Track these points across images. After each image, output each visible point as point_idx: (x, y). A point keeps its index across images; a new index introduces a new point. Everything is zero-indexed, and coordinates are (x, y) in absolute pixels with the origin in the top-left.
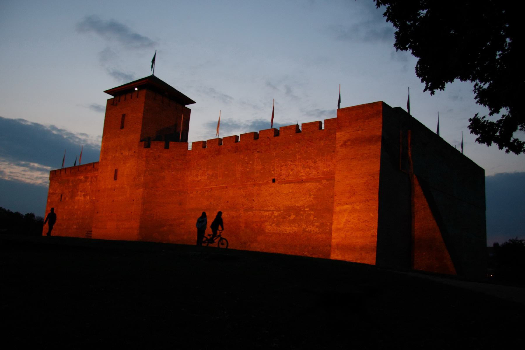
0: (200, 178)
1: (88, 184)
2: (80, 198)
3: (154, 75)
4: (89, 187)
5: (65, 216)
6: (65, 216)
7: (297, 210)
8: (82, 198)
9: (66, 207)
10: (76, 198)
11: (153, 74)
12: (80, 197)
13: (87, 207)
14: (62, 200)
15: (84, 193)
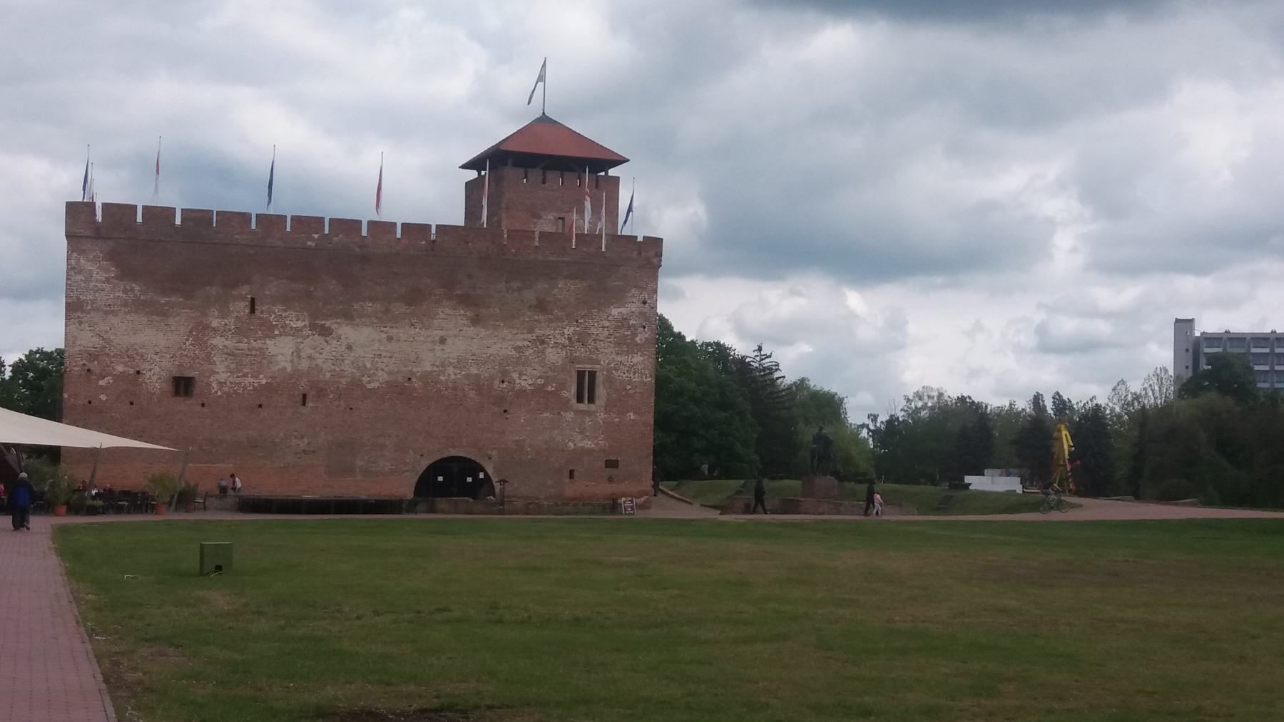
11: (544, 113)
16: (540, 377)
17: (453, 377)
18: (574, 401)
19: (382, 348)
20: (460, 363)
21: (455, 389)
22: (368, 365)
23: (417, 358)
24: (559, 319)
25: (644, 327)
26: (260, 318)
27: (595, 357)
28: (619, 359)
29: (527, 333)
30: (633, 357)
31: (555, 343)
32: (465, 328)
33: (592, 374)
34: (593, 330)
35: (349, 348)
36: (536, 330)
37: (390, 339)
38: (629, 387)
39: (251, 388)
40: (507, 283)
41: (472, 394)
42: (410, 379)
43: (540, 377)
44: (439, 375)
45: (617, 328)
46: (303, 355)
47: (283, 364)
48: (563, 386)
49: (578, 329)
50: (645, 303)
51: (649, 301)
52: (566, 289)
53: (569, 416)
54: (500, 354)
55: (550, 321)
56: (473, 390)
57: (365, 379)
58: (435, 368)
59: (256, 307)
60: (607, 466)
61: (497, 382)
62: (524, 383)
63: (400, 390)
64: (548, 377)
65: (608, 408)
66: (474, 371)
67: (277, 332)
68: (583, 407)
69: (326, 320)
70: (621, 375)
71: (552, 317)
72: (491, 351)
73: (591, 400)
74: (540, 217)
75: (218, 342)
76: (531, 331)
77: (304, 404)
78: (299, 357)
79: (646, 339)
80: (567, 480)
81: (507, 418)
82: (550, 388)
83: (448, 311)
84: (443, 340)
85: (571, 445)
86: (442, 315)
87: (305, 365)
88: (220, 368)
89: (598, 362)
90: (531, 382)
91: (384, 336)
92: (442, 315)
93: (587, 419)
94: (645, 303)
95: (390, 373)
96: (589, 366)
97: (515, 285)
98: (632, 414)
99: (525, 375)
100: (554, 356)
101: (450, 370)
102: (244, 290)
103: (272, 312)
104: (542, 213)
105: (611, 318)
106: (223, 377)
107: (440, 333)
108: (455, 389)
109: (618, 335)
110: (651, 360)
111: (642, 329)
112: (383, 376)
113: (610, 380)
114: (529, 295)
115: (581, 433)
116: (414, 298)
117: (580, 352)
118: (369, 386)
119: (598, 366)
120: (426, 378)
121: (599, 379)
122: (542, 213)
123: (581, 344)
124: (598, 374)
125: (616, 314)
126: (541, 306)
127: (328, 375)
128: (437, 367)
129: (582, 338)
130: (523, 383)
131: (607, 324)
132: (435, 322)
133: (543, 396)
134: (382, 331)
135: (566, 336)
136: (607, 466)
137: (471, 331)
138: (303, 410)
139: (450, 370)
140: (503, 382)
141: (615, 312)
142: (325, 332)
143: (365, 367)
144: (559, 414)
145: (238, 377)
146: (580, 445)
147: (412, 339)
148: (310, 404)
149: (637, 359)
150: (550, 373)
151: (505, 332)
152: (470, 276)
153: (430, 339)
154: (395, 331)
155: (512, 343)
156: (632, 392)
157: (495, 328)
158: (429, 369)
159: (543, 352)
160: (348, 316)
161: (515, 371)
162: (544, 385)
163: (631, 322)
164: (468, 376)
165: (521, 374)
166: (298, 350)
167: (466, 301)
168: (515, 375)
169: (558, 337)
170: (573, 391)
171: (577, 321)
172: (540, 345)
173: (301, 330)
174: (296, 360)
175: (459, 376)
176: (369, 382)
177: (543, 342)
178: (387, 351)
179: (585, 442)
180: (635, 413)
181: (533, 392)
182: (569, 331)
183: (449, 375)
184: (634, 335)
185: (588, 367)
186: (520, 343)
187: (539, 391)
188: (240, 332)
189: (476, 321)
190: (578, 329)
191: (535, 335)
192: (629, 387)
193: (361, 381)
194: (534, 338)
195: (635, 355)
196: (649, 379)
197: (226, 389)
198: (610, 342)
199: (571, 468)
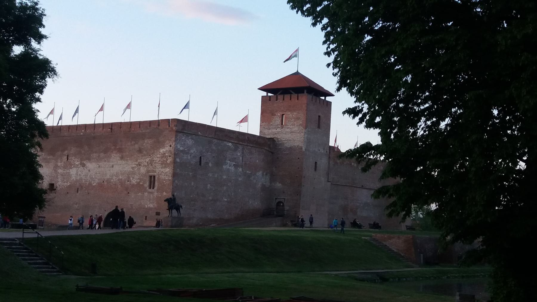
1: (239, 154)
2: (229, 166)
3: (299, 71)
4: (241, 158)
5: (209, 185)
6: (209, 185)
8: (233, 168)
9: (210, 175)
10: (224, 167)
11: (298, 71)
12: (230, 166)
13: (240, 179)
14: (202, 165)
15: (234, 163)
16: (139, 179)
17: (115, 180)
18: (148, 188)
19: (97, 170)
20: (117, 175)
21: (115, 185)
22: (94, 177)
23: (106, 173)
24: (145, 155)
25: (170, 156)
26: (69, 162)
27: (155, 170)
28: (162, 170)
29: (136, 162)
30: (166, 169)
31: (144, 165)
32: (119, 161)
33: (154, 176)
34: (155, 159)
35: (89, 171)
36: (138, 160)
37: (99, 167)
38: (164, 182)
39: (66, 187)
40: (131, 142)
41: (119, 187)
42: (104, 181)
43: (139, 179)
44: (111, 180)
45: (162, 157)
46: (78, 174)
47: (73, 178)
49: (150, 159)
50: (171, 146)
51: (172, 146)
52: (148, 143)
53: (146, 194)
54: (128, 170)
55: (142, 156)
56: (119, 185)
57: (93, 182)
58: (110, 177)
59: (68, 158)
60: (156, 215)
61: (126, 181)
62: (134, 182)
63: (101, 185)
64: (140, 179)
65: (158, 190)
66: (120, 177)
67: (72, 167)
68: (150, 190)
69: (84, 161)
70: (162, 177)
71: (143, 154)
72: (125, 169)
73: (153, 188)
74: (275, 115)
75: (60, 171)
76: (137, 161)
77: (78, 192)
78: (77, 175)
79: (171, 161)
80: (144, 220)
81: (129, 196)
82: (141, 183)
83: (114, 155)
84: (113, 166)
85: (146, 206)
86: (113, 157)
87: (78, 178)
88: (59, 180)
90: (136, 181)
91: (98, 166)
92: (113, 157)
93: (151, 195)
94: (171, 146)
95: (99, 179)
96: (153, 174)
97: (133, 143)
98: (165, 193)
99: (135, 178)
100: (143, 170)
101: (114, 178)
102: (66, 152)
103: (72, 159)
104: (276, 113)
105: (160, 153)
106: (60, 183)
107: (112, 163)
108: (115, 185)
109: (162, 160)
110: (172, 170)
111: (169, 157)
112: (97, 181)
113: (159, 179)
114: (137, 146)
115: (149, 201)
116: (106, 151)
117: (151, 168)
118: (93, 185)
119: (155, 174)
120: (108, 181)
121: (156, 178)
122: (276, 113)
123: (151, 165)
124: (156, 177)
125: (162, 151)
126: (140, 151)
127: (84, 181)
128: (111, 176)
129: (151, 163)
130: (134, 182)
131: (159, 156)
132: (111, 159)
133: (139, 187)
134: (97, 164)
135: (147, 162)
136: (156, 215)
137: (120, 162)
138: (78, 194)
139: (114, 178)
140: (128, 181)
141: (162, 151)
142: (84, 165)
143: (93, 177)
144: (143, 193)
145: (63, 183)
146: (149, 206)
147: (105, 166)
148: (79, 192)
149: (167, 170)
150: (141, 177)
151: (130, 162)
152: (121, 141)
153: (109, 166)
154: (100, 163)
155: (131, 166)
156: (165, 183)
157: (127, 160)
158: (109, 178)
159: (140, 169)
160: (89, 159)
161: (131, 177)
162: (140, 182)
163: (166, 155)
164: (119, 179)
165: (133, 178)
166: (77, 173)
167: (120, 150)
168: (131, 178)
169: (144, 162)
170: (147, 185)
171: (150, 155)
172: (139, 166)
173: (78, 165)
174: (76, 176)
175: (116, 180)
176: (93, 183)
177: (140, 165)
178: (98, 171)
179: (150, 205)
180: (166, 192)
181: (136, 185)
182: (147, 160)
183: (114, 180)
184: (167, 160)
185: (151, 174)
186: (133, 166)
187: (138, 183)
188: (65, 167)
189: (122, 158)
190: (150, 159)
191: (138, 162)
192: (164, 182)
193: (91, 183)
194: (138, 163)
195: (167, 168)
196: (171, 178)
197: (60, 187)
198: (159, 163)
199: (146, 215)
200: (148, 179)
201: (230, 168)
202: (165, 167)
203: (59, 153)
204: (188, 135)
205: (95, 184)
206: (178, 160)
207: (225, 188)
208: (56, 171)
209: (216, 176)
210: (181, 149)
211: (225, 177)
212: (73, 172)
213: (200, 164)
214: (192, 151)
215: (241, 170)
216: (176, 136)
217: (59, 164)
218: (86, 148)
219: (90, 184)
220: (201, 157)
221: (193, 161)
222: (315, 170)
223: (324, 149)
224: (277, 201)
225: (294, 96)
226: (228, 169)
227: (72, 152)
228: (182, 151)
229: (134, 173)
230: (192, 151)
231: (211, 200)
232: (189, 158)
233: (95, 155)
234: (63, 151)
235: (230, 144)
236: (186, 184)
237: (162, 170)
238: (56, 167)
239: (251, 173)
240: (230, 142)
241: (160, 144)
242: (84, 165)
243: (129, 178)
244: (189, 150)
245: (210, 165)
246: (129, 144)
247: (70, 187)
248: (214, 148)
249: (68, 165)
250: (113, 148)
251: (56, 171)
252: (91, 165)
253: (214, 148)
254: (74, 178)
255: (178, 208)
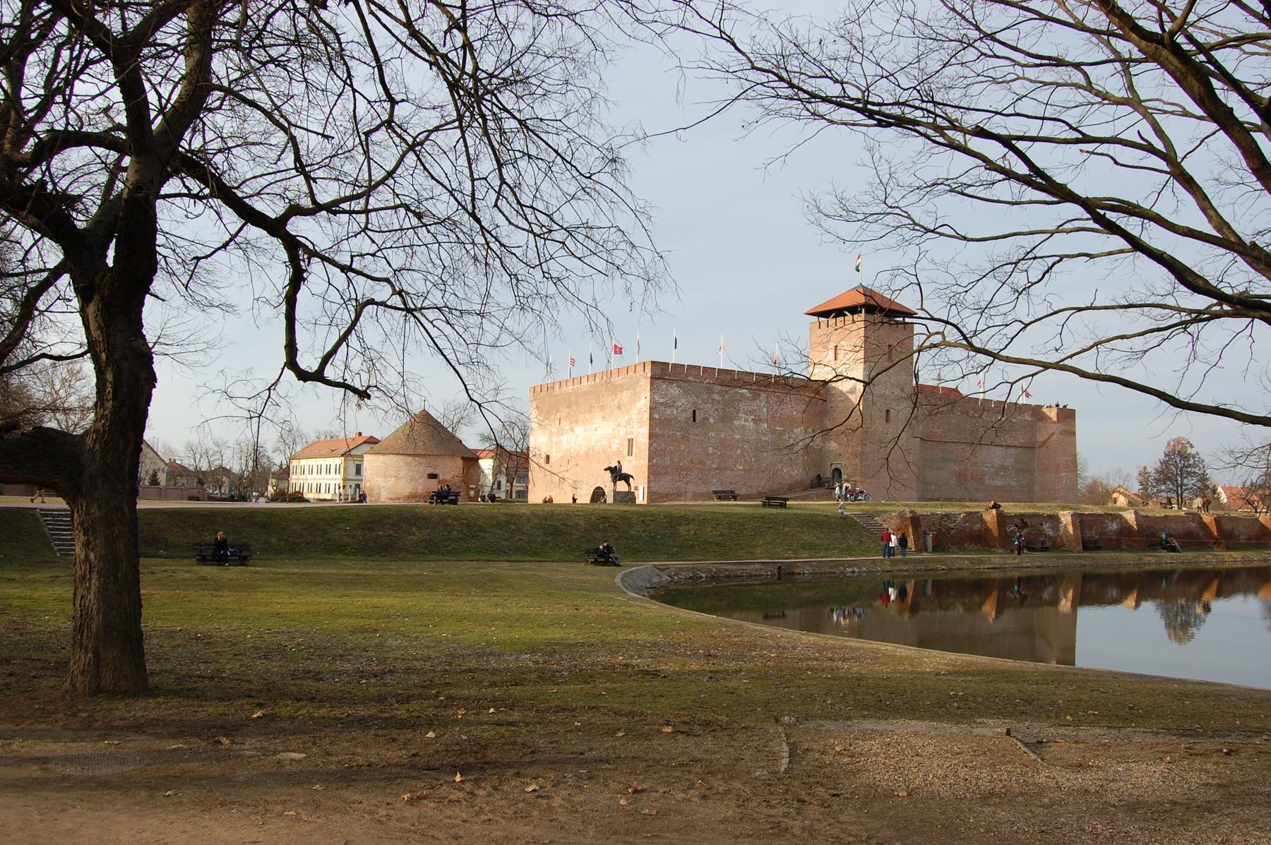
0: (936, 430)
2: (744, 421)
4: (765, 410)
7: (1004, 468)
8: (751, 425)
10: (737, 423)
14: (697, 420)
48: (624, 449)
62: (615, 448)
63: (587, 455)
66: (603, 443)
68: (629, 458)
75: (554, 439)
88: (554, 450)
89: (632, 433)
100: (622, 432)
101: (598, 444)
114: (616, 401)
126: (619, 407)
129: (628, 423)
139: (598, 444)
160: (577, 422)
167: (602, 408)
182: (626, 418)
188: (558, 433)
200: (626, 443)
201: (746, 423)
202: (641, 427)
203: (553, 416)
204: (671, 381)
205: (582, 454)
206: (656, 416)
207: (739, 452)
208: (551, 439)
209: (722, 436)
210: (661, 400)
211: (737, 437)
212: (564, 438)
213: (694, 420)
214: (679, 404)
215: (766, 426)
216: (652, 384)
217: (553, 430)
218: (574, 408)
219: (578, 454)
220: (694, 411)
221: (682, 417)
222: (887, 420)
223: (903, 390)
224: (833, 467)
225: (849, 317)
226: (743, 427)
227: (563, 415)
228: (662, 404)
229: (614, 437)
230: (679, 404)
231: (715, 469)
232: (675, 412)
233: (581, 417)
234: (556, 414)
235: (745, 391)
236: (672, 448)
237: (639, 430)
238: (551, 434)
239: (784, 431)
240: (747, 389)
241: (635, 397)
242: (572, 430)
243: (610, 443)
244: (674, 402)
245: (711, 421)
246: (610, 399)
247: (562, 458)
248: (717, 397)
249: (560, 432)
250: (596, 405)
251: (551, 439)
252: (579, 429)
253: (717, 397)
254: (565, 446)
255: (626, 478)
